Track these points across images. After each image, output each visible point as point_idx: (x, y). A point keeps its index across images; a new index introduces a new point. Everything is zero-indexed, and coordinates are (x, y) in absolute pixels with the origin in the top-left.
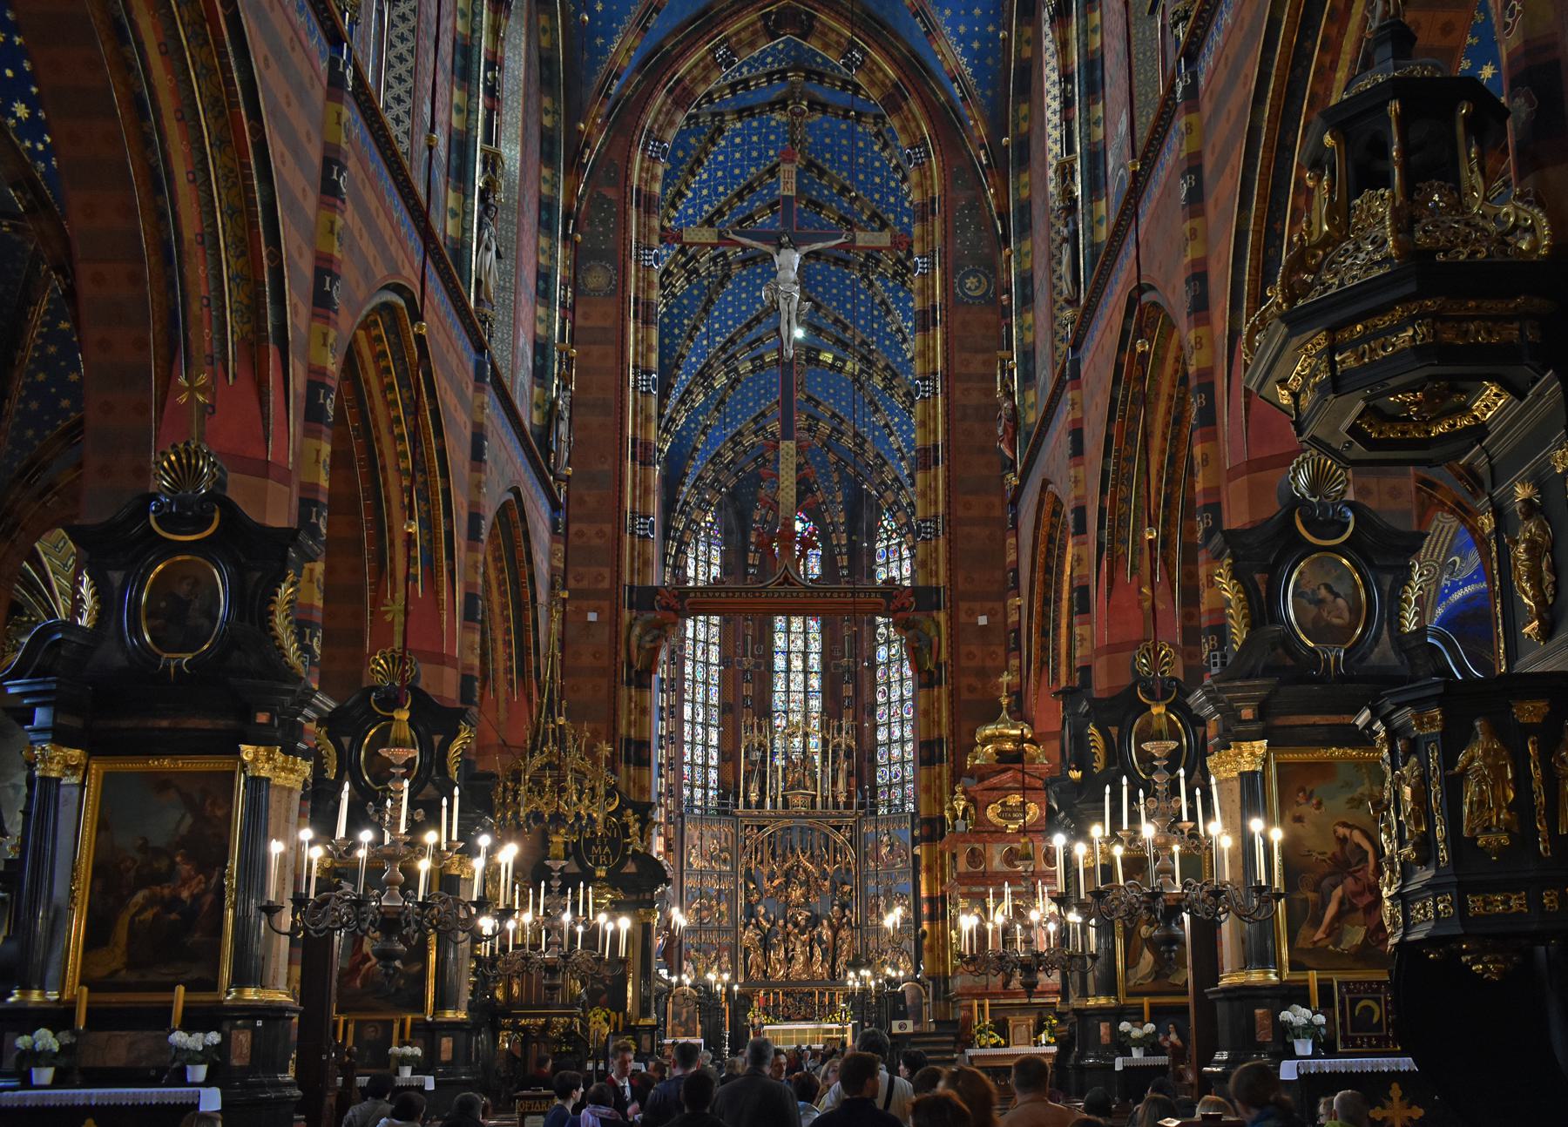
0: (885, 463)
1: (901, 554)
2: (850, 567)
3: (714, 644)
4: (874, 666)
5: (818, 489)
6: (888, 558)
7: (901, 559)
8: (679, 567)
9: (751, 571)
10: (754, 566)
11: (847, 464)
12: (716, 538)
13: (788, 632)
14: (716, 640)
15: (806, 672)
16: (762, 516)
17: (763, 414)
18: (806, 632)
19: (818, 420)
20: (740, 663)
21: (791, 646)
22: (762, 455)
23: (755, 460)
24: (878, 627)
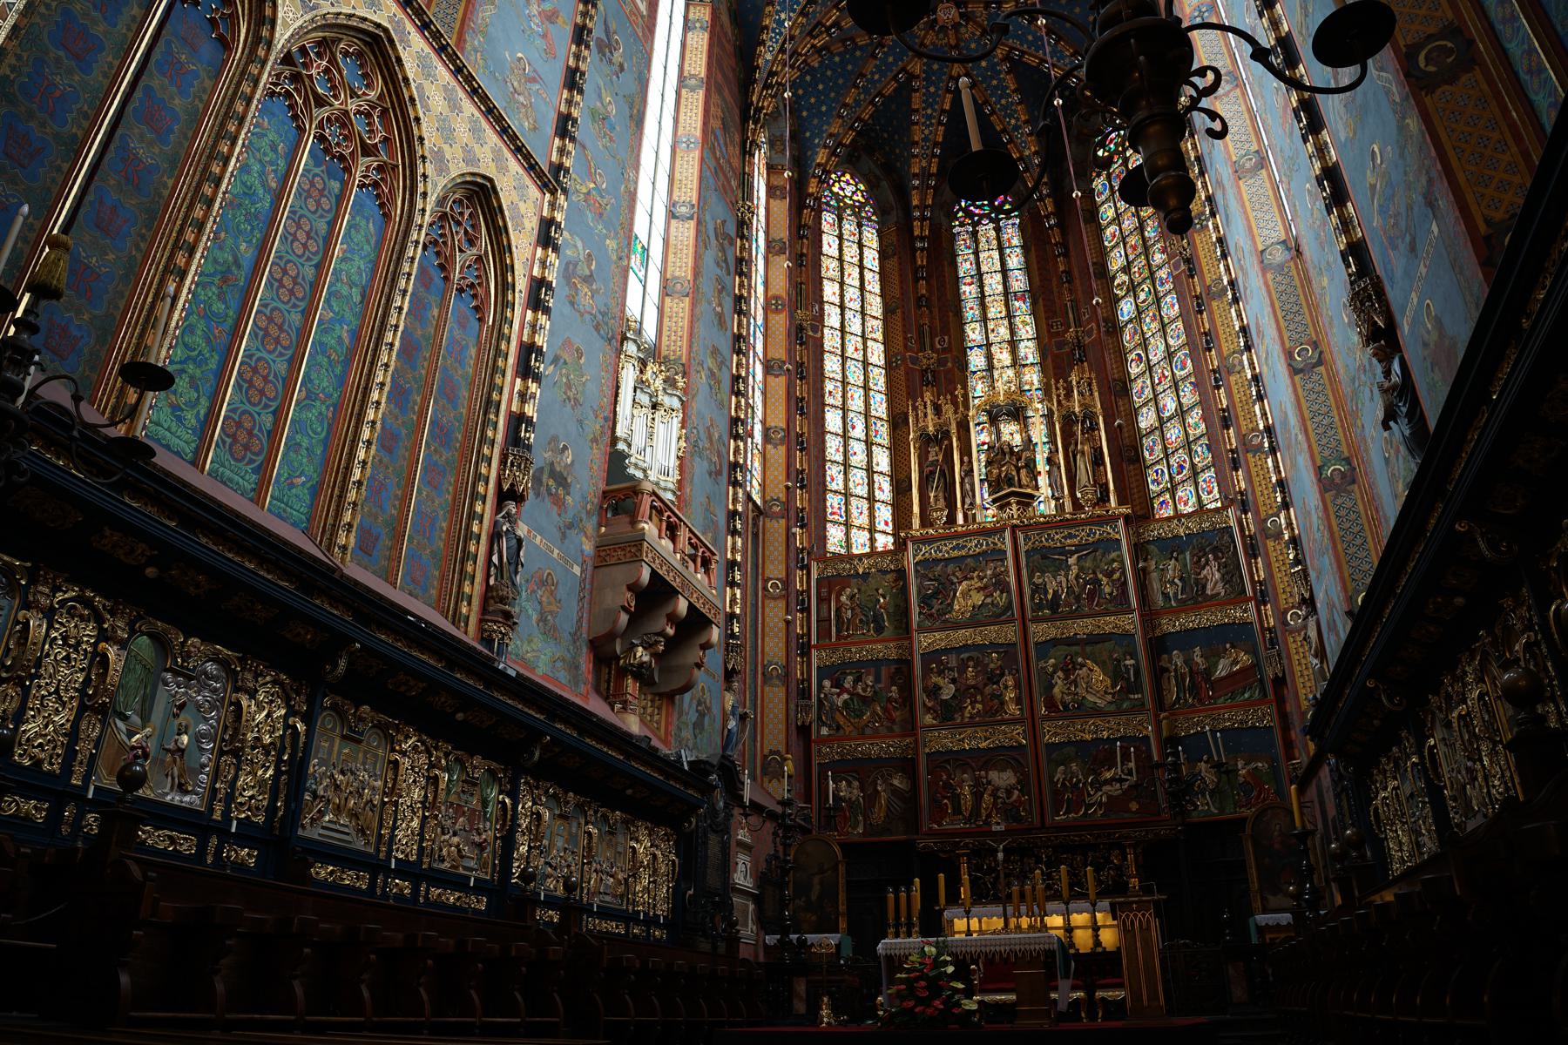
4: (1115, 329)
5: (993, 112)
9: (919, 245)
10: (922, 239)
11: (1023, 53)
12: (869, 219)
13: (984, 319)
14: (879, 336)
15: (1016, 363)
16: (923, 169)
18: (1010, 316)
20: (915, 361)
21: (991, 336)
22: (903, 70)
23: (895, 78)
24: (1114, 278)
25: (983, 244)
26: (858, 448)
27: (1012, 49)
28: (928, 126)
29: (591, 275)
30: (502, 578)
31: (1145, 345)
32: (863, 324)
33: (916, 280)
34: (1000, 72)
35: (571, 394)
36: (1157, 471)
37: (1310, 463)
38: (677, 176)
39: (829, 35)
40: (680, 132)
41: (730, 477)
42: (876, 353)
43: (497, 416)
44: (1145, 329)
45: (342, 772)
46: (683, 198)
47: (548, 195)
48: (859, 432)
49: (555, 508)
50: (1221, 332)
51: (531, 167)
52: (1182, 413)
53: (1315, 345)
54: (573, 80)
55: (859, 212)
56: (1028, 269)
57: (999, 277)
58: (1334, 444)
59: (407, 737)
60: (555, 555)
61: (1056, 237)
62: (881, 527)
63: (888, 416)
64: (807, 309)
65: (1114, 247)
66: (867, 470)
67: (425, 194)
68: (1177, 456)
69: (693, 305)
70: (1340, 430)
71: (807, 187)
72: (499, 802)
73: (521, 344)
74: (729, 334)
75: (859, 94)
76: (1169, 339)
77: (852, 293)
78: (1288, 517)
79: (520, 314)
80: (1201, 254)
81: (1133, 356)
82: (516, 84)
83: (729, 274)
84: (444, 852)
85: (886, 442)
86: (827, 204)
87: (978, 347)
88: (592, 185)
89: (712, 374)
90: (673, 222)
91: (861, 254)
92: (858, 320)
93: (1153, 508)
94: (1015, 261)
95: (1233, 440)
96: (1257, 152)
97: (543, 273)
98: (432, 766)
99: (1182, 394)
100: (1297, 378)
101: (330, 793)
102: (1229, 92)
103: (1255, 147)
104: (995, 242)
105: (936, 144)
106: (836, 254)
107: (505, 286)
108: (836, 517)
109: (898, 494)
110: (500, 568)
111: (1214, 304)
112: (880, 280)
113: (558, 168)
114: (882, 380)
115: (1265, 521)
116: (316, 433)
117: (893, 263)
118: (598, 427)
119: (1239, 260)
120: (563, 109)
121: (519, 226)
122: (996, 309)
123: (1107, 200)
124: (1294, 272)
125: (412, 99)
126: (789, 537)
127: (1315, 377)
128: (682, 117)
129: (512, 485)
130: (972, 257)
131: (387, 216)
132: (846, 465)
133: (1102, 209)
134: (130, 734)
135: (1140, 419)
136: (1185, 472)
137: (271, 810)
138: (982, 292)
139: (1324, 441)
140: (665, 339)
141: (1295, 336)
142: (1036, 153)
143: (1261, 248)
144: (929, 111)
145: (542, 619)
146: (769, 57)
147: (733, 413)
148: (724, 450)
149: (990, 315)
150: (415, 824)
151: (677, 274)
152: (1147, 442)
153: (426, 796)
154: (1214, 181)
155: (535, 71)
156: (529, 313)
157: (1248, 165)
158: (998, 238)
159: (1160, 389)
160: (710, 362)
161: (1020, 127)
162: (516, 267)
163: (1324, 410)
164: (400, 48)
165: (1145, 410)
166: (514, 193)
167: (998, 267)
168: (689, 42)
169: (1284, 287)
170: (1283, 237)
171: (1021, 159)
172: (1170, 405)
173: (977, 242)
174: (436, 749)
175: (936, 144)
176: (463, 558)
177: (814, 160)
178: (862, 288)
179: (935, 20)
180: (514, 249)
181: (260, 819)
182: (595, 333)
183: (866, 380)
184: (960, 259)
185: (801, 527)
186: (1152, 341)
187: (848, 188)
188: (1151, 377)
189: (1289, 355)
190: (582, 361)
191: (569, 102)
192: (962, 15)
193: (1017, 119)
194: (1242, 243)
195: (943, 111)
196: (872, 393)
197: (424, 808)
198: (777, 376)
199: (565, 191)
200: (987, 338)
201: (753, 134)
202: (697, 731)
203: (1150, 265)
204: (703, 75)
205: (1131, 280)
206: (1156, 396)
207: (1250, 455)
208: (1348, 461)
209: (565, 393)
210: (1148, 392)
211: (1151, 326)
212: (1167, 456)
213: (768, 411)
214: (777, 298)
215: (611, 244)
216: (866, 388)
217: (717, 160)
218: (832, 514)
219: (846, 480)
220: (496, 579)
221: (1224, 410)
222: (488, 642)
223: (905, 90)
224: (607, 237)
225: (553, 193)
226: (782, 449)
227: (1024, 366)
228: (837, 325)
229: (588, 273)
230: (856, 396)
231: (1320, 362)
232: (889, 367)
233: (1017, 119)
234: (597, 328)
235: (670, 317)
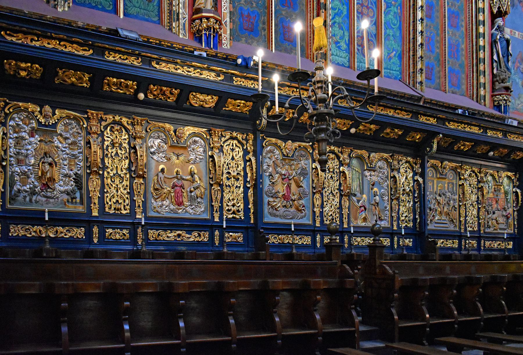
30: (501, 68)
45: (440, 196)
59: (466, 170)
72: (514, 192)
84: (490, 223)
98: (479, 182)
101: (436, 206)
134: (358, 201)
137: (415, 220)
150: (475, 212)
153: (478, 198)
174: (480, 173)
176: (477, 62)
181: (411, 225)
197: (478, 203)
222: (498, 107)
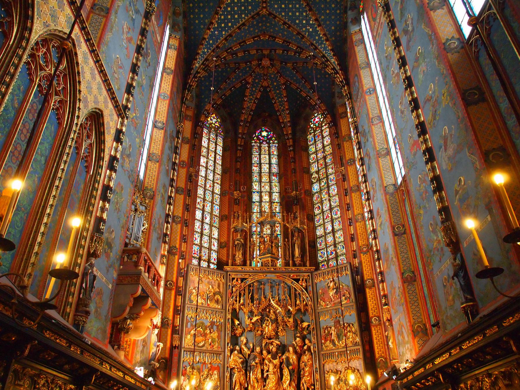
0: (316, 48)
1: (322, 136)
2: (294, 146)
3: (218, 183)
4: (310, 194)
5: (275, 103)
6: (315, 140)
7: (323, 138)
8: (197, 133)
9: (239, 148)
10: (241, 146)
11: (291, 83)
12: (220, 134)
13: (260, 182)
14: (219, 182)
17: (244, 24)
18: (270, 182)
19: (275, 38)
20: (233, 194)
21: (262, 189)
22: (244, 79)
24: (312, 175)
25: (263, 152)
26: (207, 227)
27: (287, 81)
28: (250, 103)
29: (130, 154)
30: (86, 295)
31: (322, 202)
32: (214, 176)
33: (237, 162)
34: (281, 88)
35: (117, 207)
36: (322, 253)
37: (398, 270)
38: (158, 110)
39: (221, 61)
40: (161, 91)
41: (163, 240)
42: (217, 189)
43: (91, 218)
44: (323, 197)
46: (160, 120)
47: (120, 119)
48: (207, 220)
49: (107, 259)
50: (354, 205)
51: (116, 106)
52: (333, 231)
53: (403, 226)
54: (134, 69)
55: (217, 130)
56: (279, 165)
57: (267, 166)
58: (409, 265)
60: (104, 281)
61: (292, 155)
62: (213, 261)
63: (219, 215)
64: (194, 168)
65: (313, 163)
66: (209, 237)
67: (78, 117)
68: (330, 248)
69: (160, 166)
70: (411, 260)
71: (201, 118)
73: (104, 184)
74: (169, 178)
75: (226, 85)
76: (332, 203)
77: (211, 163)
78: (383, 286)
79: (105, 172)
80: (350, 174)
81: (317, 206)
82: (115, 69)
83: (172, 153)
85: (217, 226)
86: (205, 125)
87: (257, 192)
88: (134, 115)
89: (162, 195)
90: (155, 129)
91: (216, 148)
92: (212, 175)
93: (319, 266)
94: (274, 161)
95: (355, 247)
96: (386, 148)
97: (116, 154)
99: (335, 224)
100: (396, 237)
102: (378, 123)
103: (386, 147)
104: (267, 152)
105: (252, 110)
106: (206, 146)
107: (100, 158)
108: (196, 255)
109: (220, 248)
110: (85, 290)
111: (353, 194)
112: (222, 159)
113: (126, 107)
114: (219, 200)
115: (366, 281)
116: (18, 227)
117: (228, 153)
118: (125, 221)
119: (373, 186)
120: (129, 81)
121: (109, 132)
122: (265, 179)
123: (312, 144)
124: (397, 197)
125: (79, 73)
126: (179, 263)
127: (402, 238)
128: (163, 85)
129: (95, 251)
130: (258, 156)
131: (60, 124)
132: (202, 234)
133: (310, 147)
135: (317, 231)
136: (333, 255)
138: (261, 171)
139: (405, 263)
140: (147, 179)
141: (396, 221)
142: (289, 121)
143: (385, 185)
144: (251, 97)
145: (96, 311)
146: (197, 65)
147: (167, 212)
148: (162, 228)
149: (263, 180)
151: (155, 152)
152: (319, 240)
154: (365, 152)
155: (122, 64)
156: (108, 171)
157: (383, 153)
158: (269, 150)
159: (326, 221)
160: (162, 191)
161: (284, 110)
162: (106, 150)
163: (405, 251)
164: (77, 49)
165: (319, 228)
166: (109, 117)
167: (268, 162)
168: (169, 53)
169: (393, 202)
170: (394, 183)
171: (283, 122)
172: (330, 228)
173: (260, 150)
175: (252, 110)
177: (204, 107)
178: (215, 162)
179: (261, 64)
180: (106, 142)
182: (128, 179)
183: (213, 200)
184: (253, 156)
185: (182, 259)
186: (325, 202)
187: (213, 120)
188: (323, 216)
189: (393, 228)
190: (123, 192)
191: (133, 79)
192: (271, 64)
193: (284, 107)
194: (376, 180)
195: (256, 98)
196: (214, 205)
198: (180, 194)
199: (127, 118)
200: (261, 189)
201: (187, 95)
202: (142, 354)
203: (326, 172)
204: (173, 69)
205: (319, 177)
206: (324, 223)
207: (362, 255)
208: (413, 272)
209: (116, 206)
210: (321, 221)
211: (325, 196)
212: (327, 247)
213: (175, 209)
214: (183, 162)
215: (138, 140)
216: (212, 203)
217: (173, 105)
218: (194, 254)
219: (201, 240)
220: (83, 295)
221: (352, 235)
223: (244, 88)
224: (137, 137)
225: (123, 118)
226: (179, 226)
227: (274, 203)
228: (204, 175)
229: (129, 153)
230: (208, 205)
231: (405, 233)
232: (222, 195)
233: (284, 107)
234: (129, 177)
235: (150, 170)
